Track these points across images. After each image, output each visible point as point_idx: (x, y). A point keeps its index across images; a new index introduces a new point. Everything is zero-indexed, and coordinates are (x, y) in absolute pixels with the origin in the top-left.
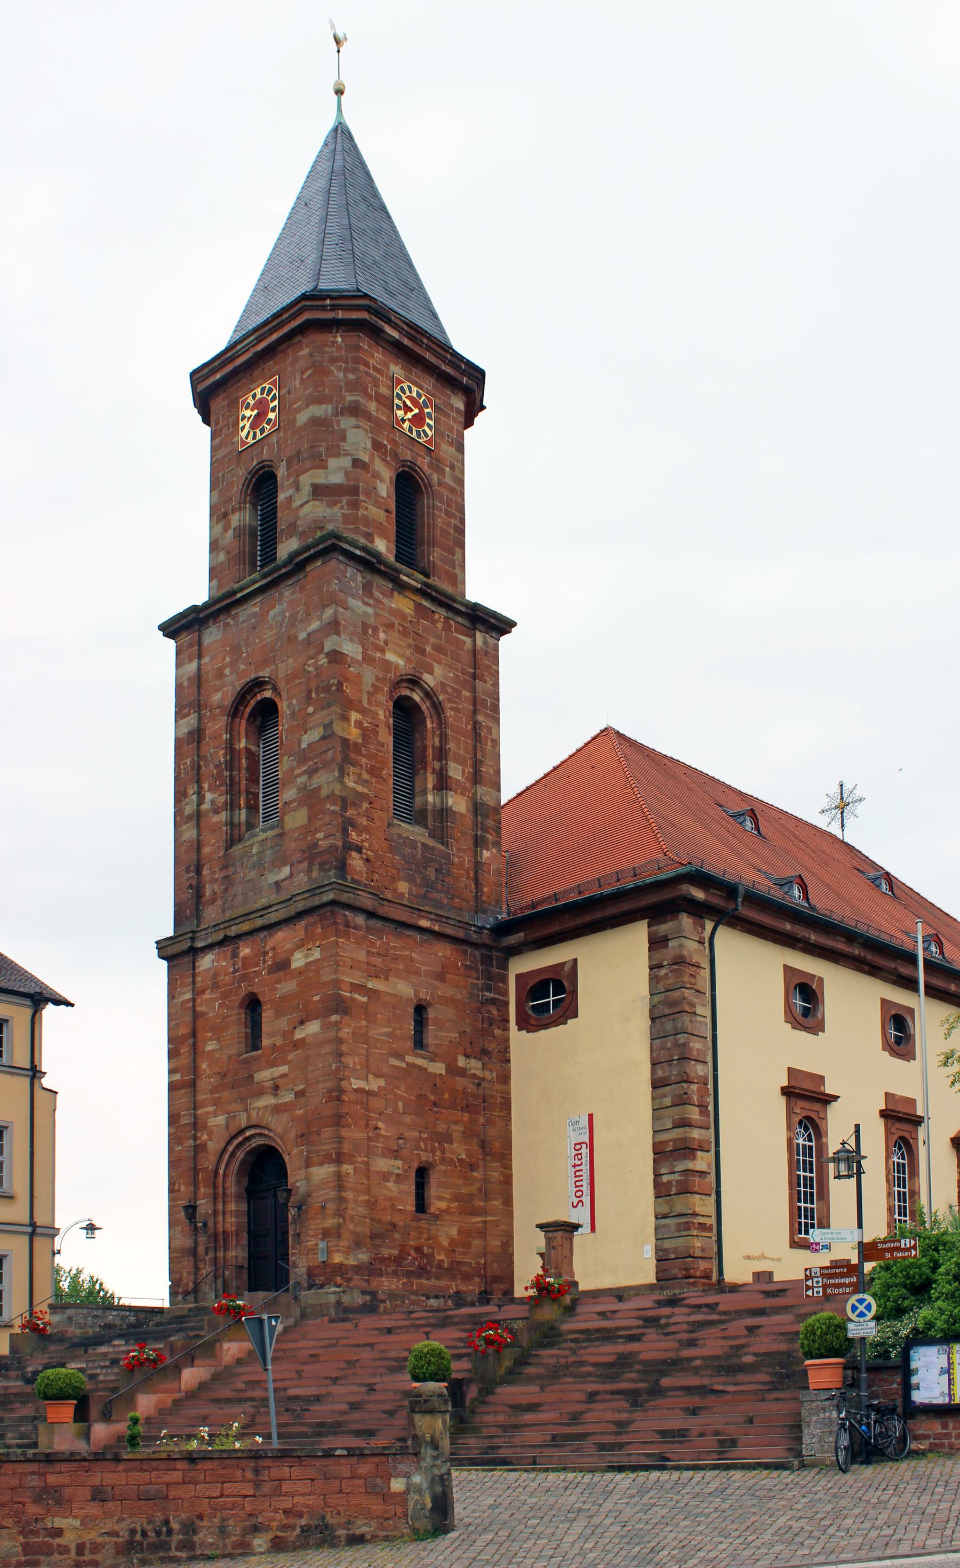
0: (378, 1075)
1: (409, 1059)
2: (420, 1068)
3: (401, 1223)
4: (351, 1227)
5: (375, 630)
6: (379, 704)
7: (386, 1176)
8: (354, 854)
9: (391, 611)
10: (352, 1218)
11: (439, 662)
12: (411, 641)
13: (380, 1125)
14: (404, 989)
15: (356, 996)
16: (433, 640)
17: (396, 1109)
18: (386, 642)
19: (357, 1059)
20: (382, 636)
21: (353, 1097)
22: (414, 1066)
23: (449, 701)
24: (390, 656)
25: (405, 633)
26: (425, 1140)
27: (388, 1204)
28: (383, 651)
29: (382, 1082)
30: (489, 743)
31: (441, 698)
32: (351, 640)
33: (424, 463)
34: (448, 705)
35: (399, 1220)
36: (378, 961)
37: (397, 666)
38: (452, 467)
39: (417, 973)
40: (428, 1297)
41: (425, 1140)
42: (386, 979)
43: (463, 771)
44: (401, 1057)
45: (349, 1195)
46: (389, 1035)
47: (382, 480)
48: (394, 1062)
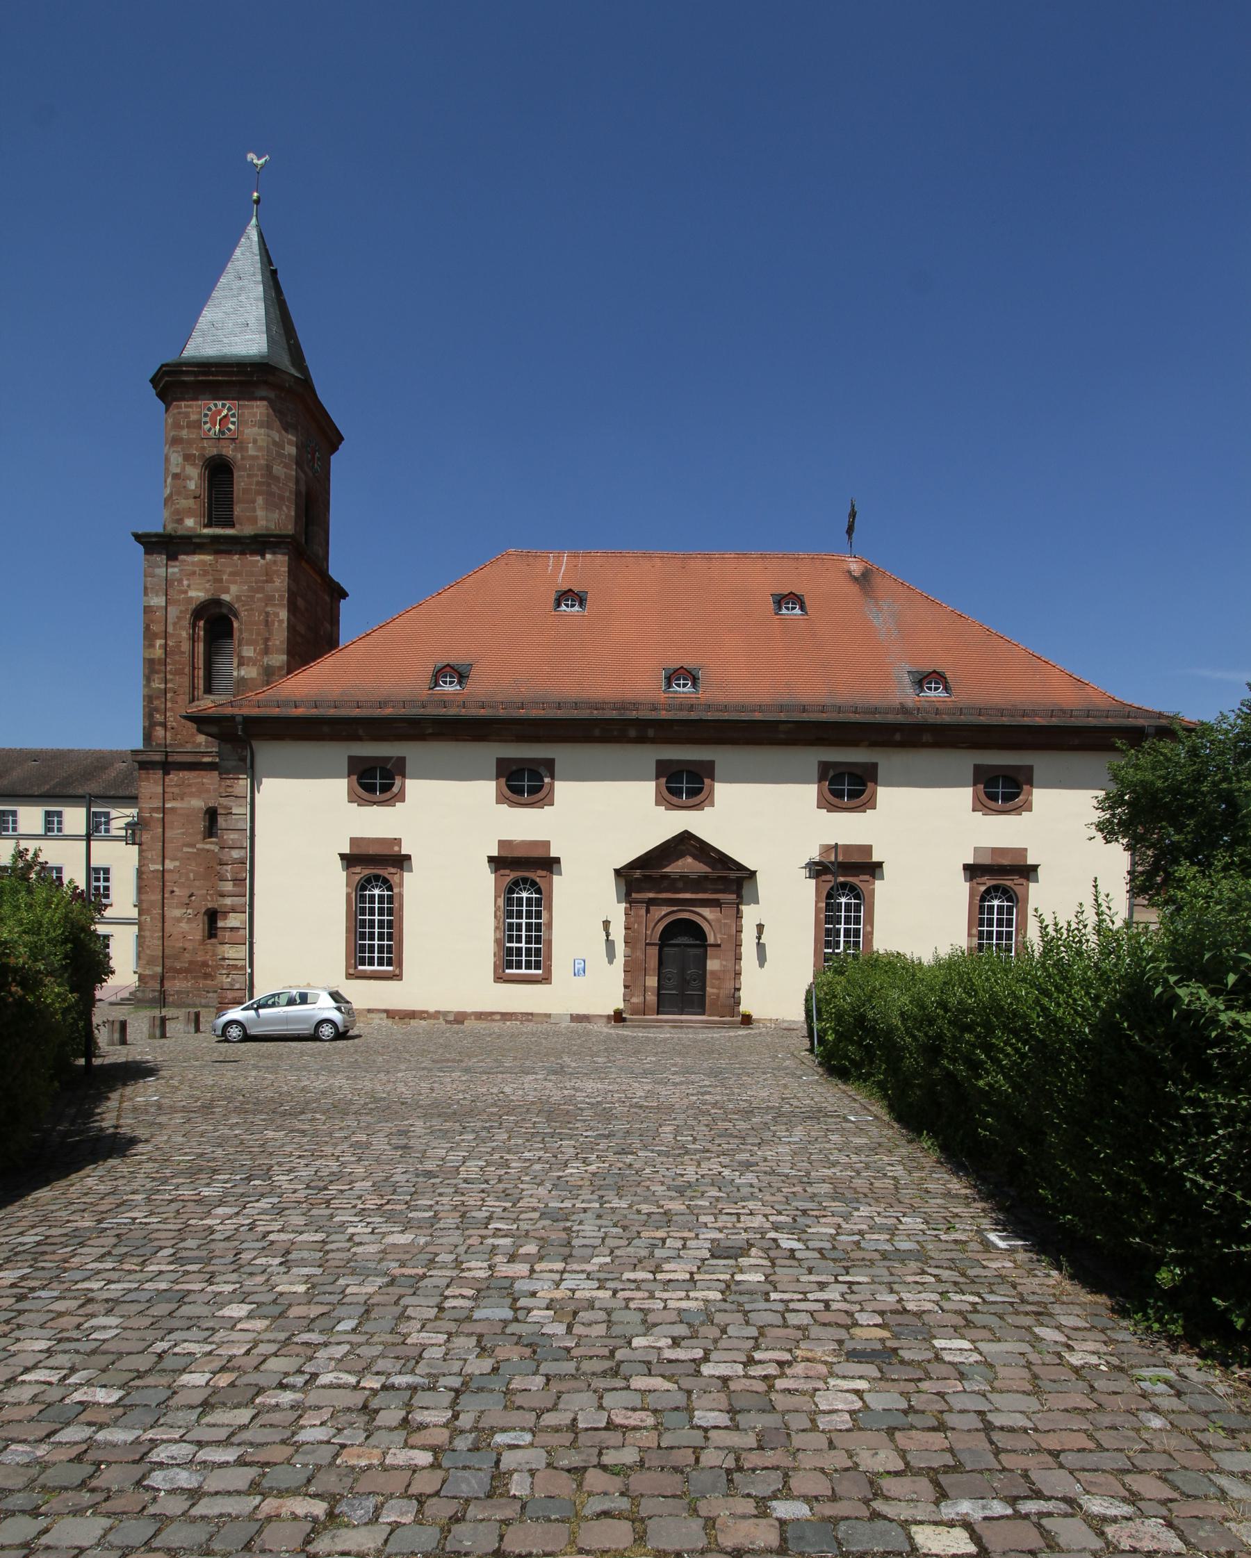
0: (173, 859)
1: (198, 846)
2: (208, 851)
3: (191, 948)
4: (148, 952)
5: (180, 581)
6: (181, 628)
7: (179, 920)
8: (158, 728)
9: (193, 563)
10: (149, 947)
11: (235, 582)
12: (211, 578)
13: (175, 889)
14: (198, 804)
15: (155, 815)
16: (229, 570)
17: (188, 879)
18: (189, 586)
19: (154, 853)
20: (185, 583)
21: (151, 876)
22: (203, 850)
23: (243, 606)
24: (192, 594)
25: (205, 573)
26: (211, 895)
27: (181, 936)
28: (186, 592)
29: (177, 863)
30: (276, 624)
31: (236, 606)
32: (157, 596)
33: (229, 451)
34: (242, 609)
35: (189, 945)
36: (176, 790)
37: (198, 598)
38: (255, 441)
39: (208, 791)
40: (208, 992)
41: (211, 895)
42: (182, 799)
43: (255, 650)
44: (193, 846)
45: (147, 934)
46: (183, 834)
47: (190, 479)
48: (186, 849)
